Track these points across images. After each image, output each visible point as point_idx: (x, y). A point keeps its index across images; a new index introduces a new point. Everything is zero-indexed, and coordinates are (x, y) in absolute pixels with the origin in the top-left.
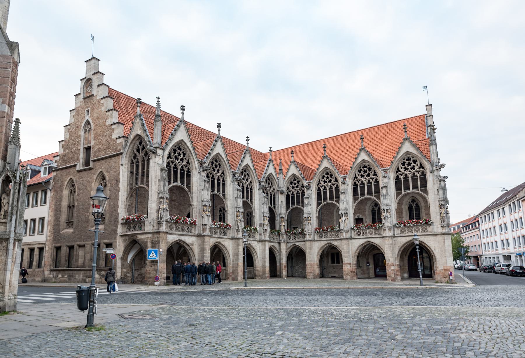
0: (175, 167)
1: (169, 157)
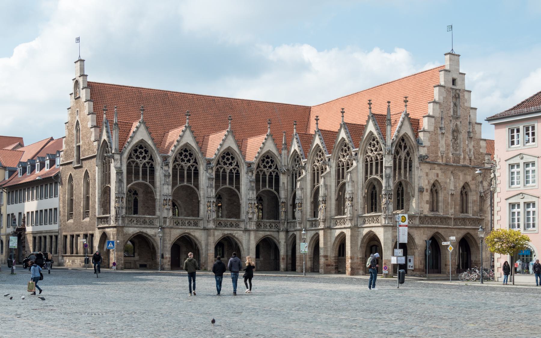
0: (137, 165)
1: (130, 157)
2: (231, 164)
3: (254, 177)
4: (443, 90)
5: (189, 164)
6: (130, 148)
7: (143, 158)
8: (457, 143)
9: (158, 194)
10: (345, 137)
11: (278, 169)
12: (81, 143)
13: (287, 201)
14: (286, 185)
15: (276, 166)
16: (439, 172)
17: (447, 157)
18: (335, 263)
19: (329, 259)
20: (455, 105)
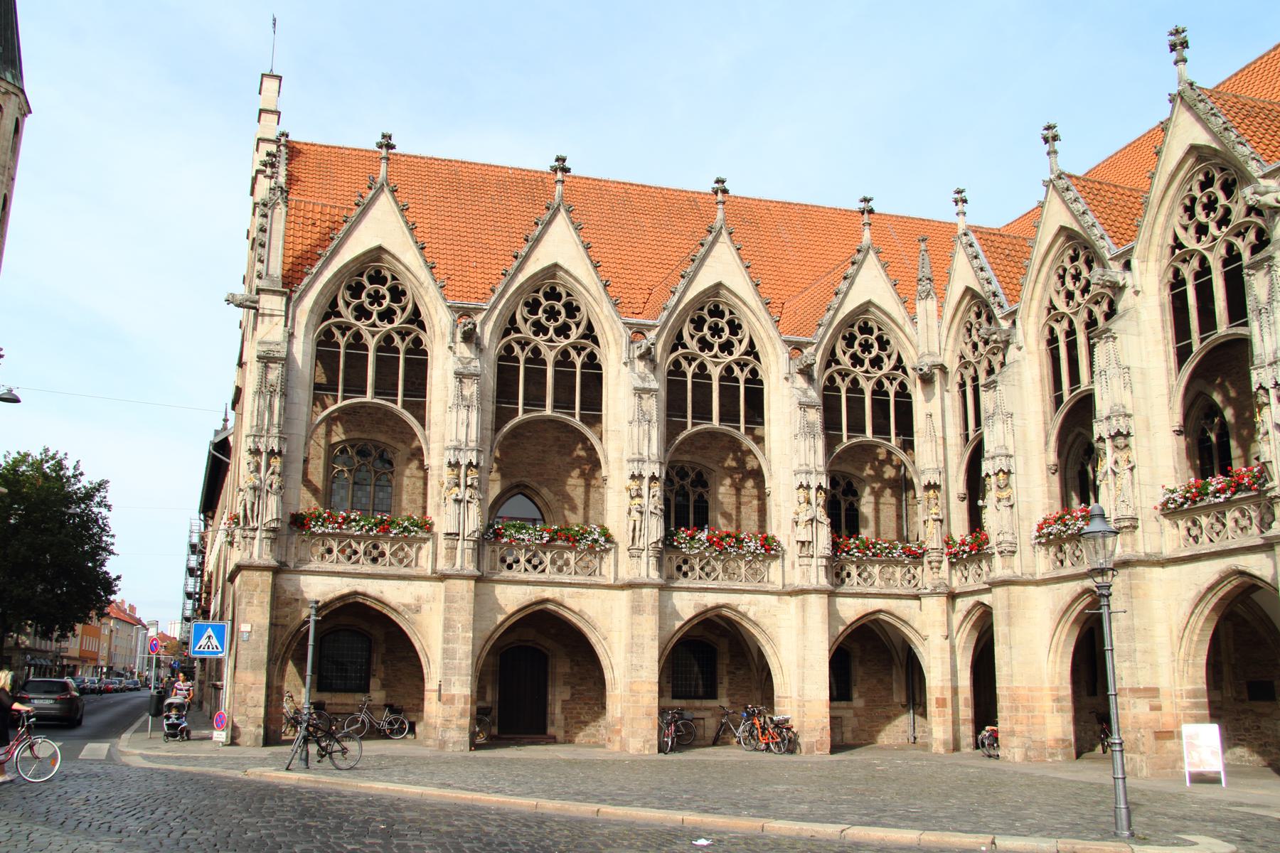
3: (814, 395)
5: (562, 342)
7: (382, 316)
11: (905, 372)
13: (946, 481)
14: (938, 424)
15: (899, 359)
19: (1166, 703)
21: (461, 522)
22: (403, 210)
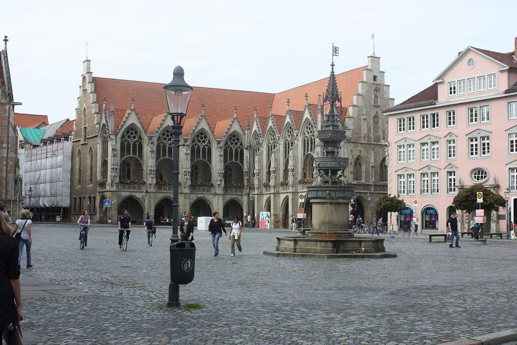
0: (129, 144)
1: (123, 137)
2: (204, 142)
4: (365, 85)
6: (123, 130)
7: (133, 137)
8: (378, 126)
9: (145, 165)
10: (290, 121)
12: (87, 126)
16: (362, 149)
17: (369, 137)
18: (283, 220)
20: (376, 97)
21: (152, 181)
22: (137, 114)
